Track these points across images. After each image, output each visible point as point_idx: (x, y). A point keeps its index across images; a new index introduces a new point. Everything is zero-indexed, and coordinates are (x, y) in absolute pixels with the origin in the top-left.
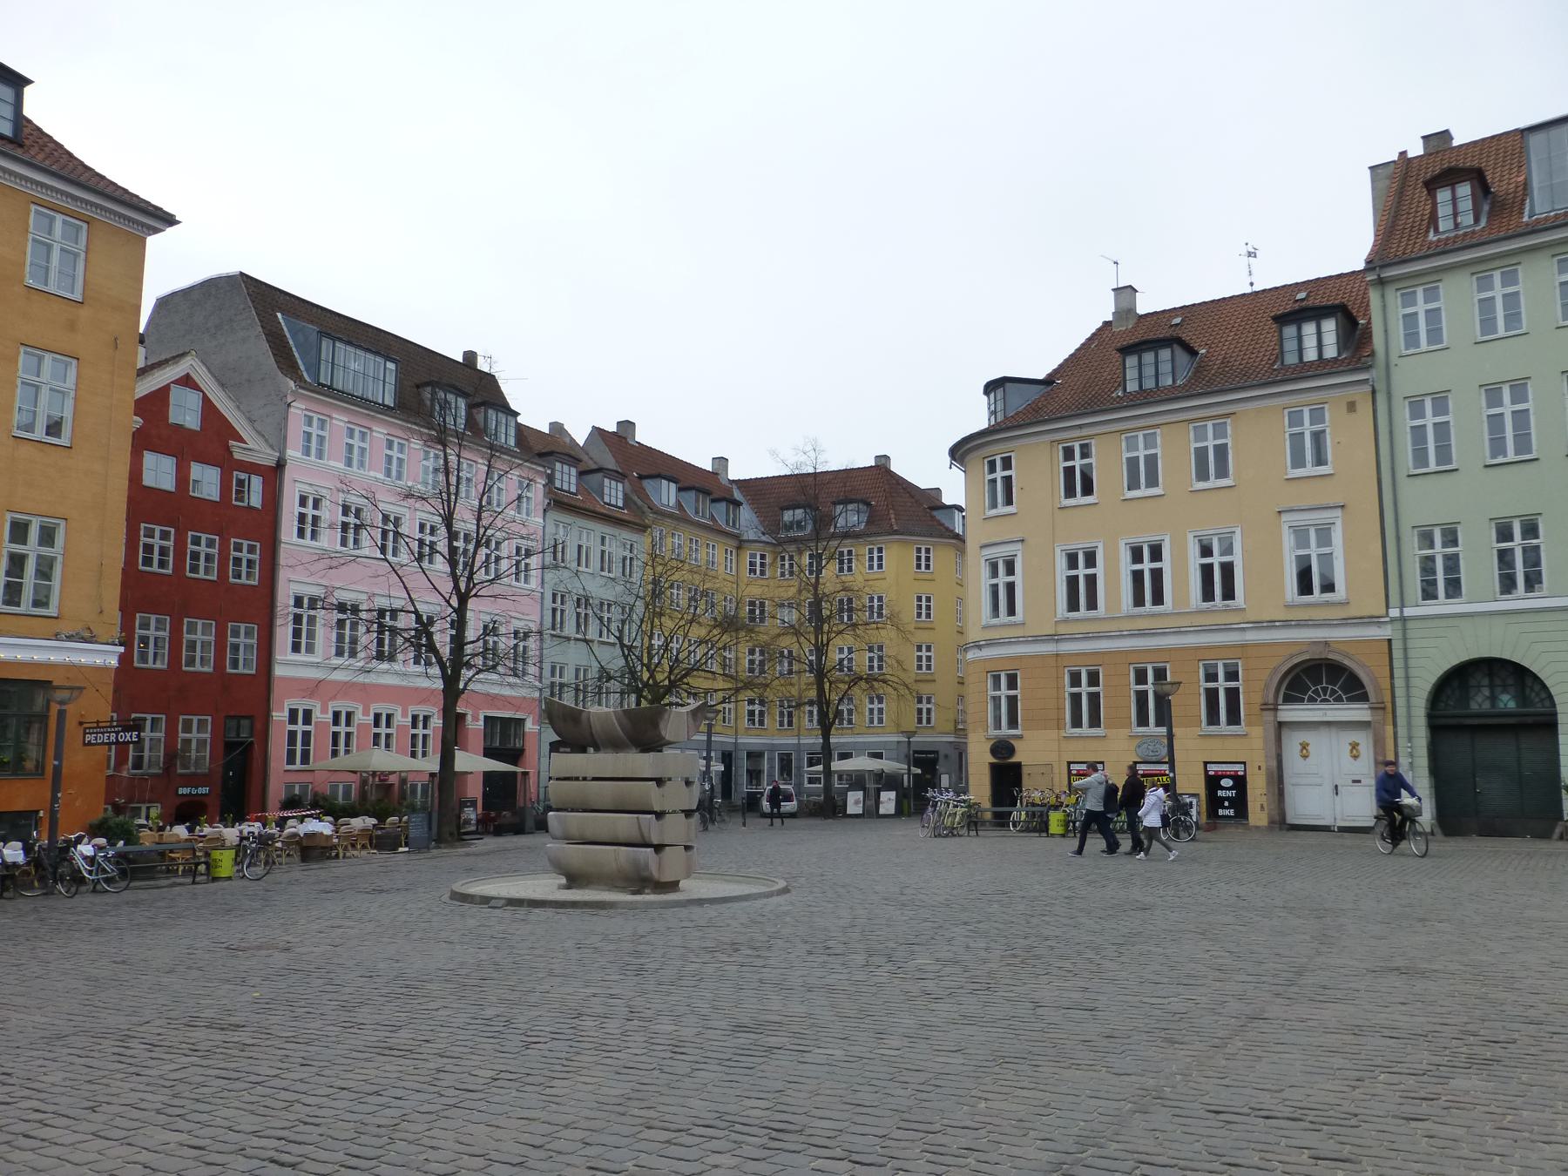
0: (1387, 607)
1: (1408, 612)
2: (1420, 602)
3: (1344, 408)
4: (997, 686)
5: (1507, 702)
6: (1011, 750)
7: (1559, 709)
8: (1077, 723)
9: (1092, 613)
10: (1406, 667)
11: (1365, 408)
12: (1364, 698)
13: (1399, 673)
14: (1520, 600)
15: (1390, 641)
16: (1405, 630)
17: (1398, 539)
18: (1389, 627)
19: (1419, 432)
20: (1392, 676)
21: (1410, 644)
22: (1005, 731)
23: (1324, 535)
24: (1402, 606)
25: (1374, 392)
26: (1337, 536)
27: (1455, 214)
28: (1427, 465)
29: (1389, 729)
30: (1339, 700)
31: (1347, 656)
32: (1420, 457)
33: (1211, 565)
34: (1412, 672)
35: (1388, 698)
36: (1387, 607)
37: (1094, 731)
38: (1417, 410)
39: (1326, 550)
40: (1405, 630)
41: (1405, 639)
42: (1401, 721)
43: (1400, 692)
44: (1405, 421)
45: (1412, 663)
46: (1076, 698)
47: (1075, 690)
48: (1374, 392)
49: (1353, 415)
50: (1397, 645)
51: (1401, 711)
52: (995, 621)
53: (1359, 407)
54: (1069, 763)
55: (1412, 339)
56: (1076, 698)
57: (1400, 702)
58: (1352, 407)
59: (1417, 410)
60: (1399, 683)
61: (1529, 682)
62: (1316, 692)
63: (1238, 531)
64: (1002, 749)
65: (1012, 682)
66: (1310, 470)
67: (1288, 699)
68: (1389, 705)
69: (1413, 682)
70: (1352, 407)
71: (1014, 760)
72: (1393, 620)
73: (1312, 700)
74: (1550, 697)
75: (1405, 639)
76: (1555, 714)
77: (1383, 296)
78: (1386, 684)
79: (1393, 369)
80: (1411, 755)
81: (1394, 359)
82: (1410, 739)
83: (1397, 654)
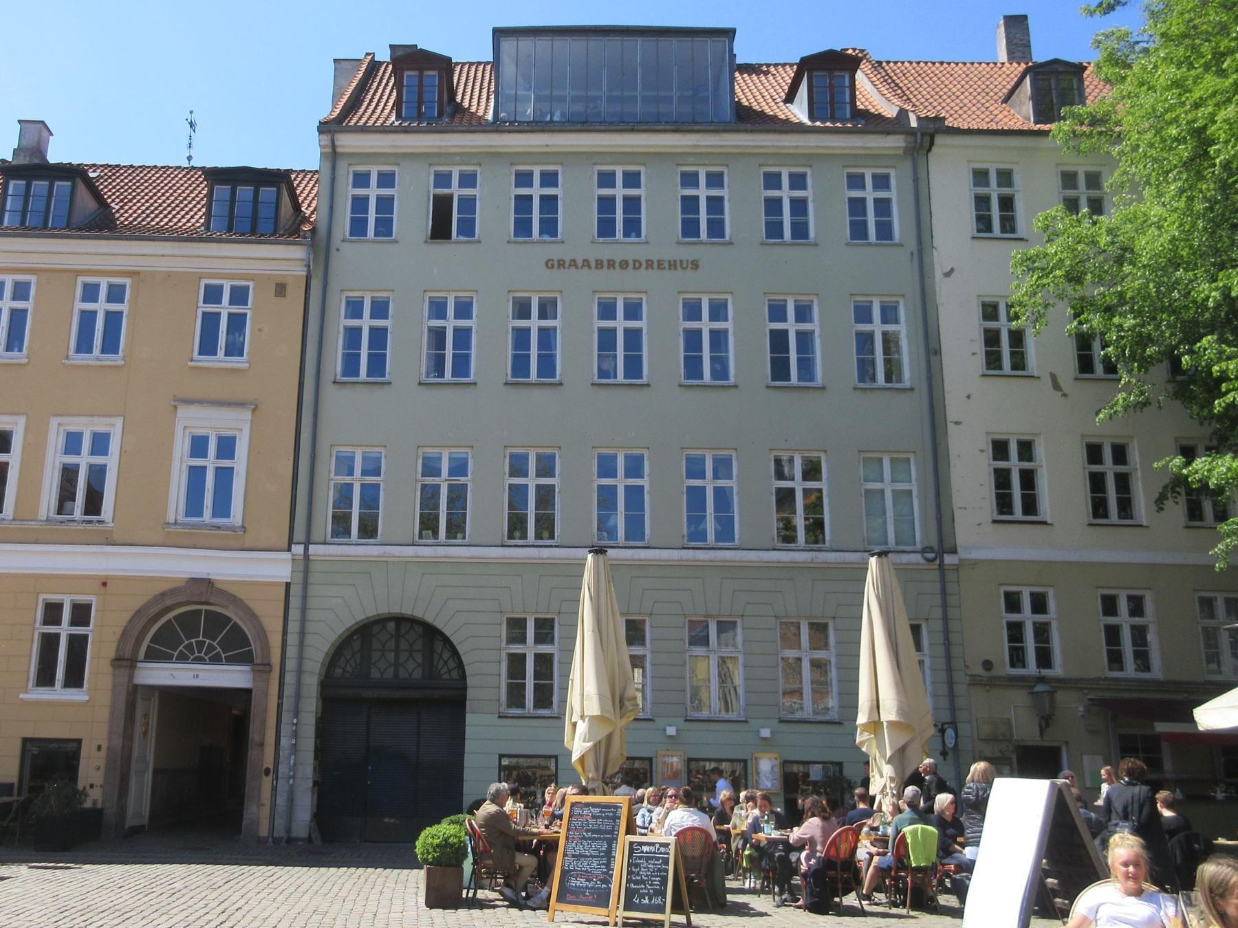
0: (291, 542)
3: (273, 288)
5: (413, 669)
7: (470, 681)
12: (244, 658)
13: (294, 627)
14: (439, 551)
15: (288, 585)
16: (307, 572)
19: (353, 336)
21: (312, 590)
23: (227, 447)
24: (307, 543)
25: (308, 278)
27: (420, 103)
28: (358, 375)
30: (216, 660)
31: (234, 600)
32: (351, 364)
34: (310, 627)
35: (276, 659)
36: (291, 542)
38: (355, 309)
39: (225, 463)
40: (307, 572)
41: (305, 584)
45: (311, 615)
50: (296, 591)
53: (289, 291)
55: (358, 227)
59: (355, 309)
61: (439, 646)
69: (309, 639)
70: (281, 290)
73: (182, 658)
74: (461, 666)
75: (305, 584)
76: (465, 688)
78: (275, 641)
79: (333, 250)
80: (295, 734)
82: (296, 713)
83: (295, 602)
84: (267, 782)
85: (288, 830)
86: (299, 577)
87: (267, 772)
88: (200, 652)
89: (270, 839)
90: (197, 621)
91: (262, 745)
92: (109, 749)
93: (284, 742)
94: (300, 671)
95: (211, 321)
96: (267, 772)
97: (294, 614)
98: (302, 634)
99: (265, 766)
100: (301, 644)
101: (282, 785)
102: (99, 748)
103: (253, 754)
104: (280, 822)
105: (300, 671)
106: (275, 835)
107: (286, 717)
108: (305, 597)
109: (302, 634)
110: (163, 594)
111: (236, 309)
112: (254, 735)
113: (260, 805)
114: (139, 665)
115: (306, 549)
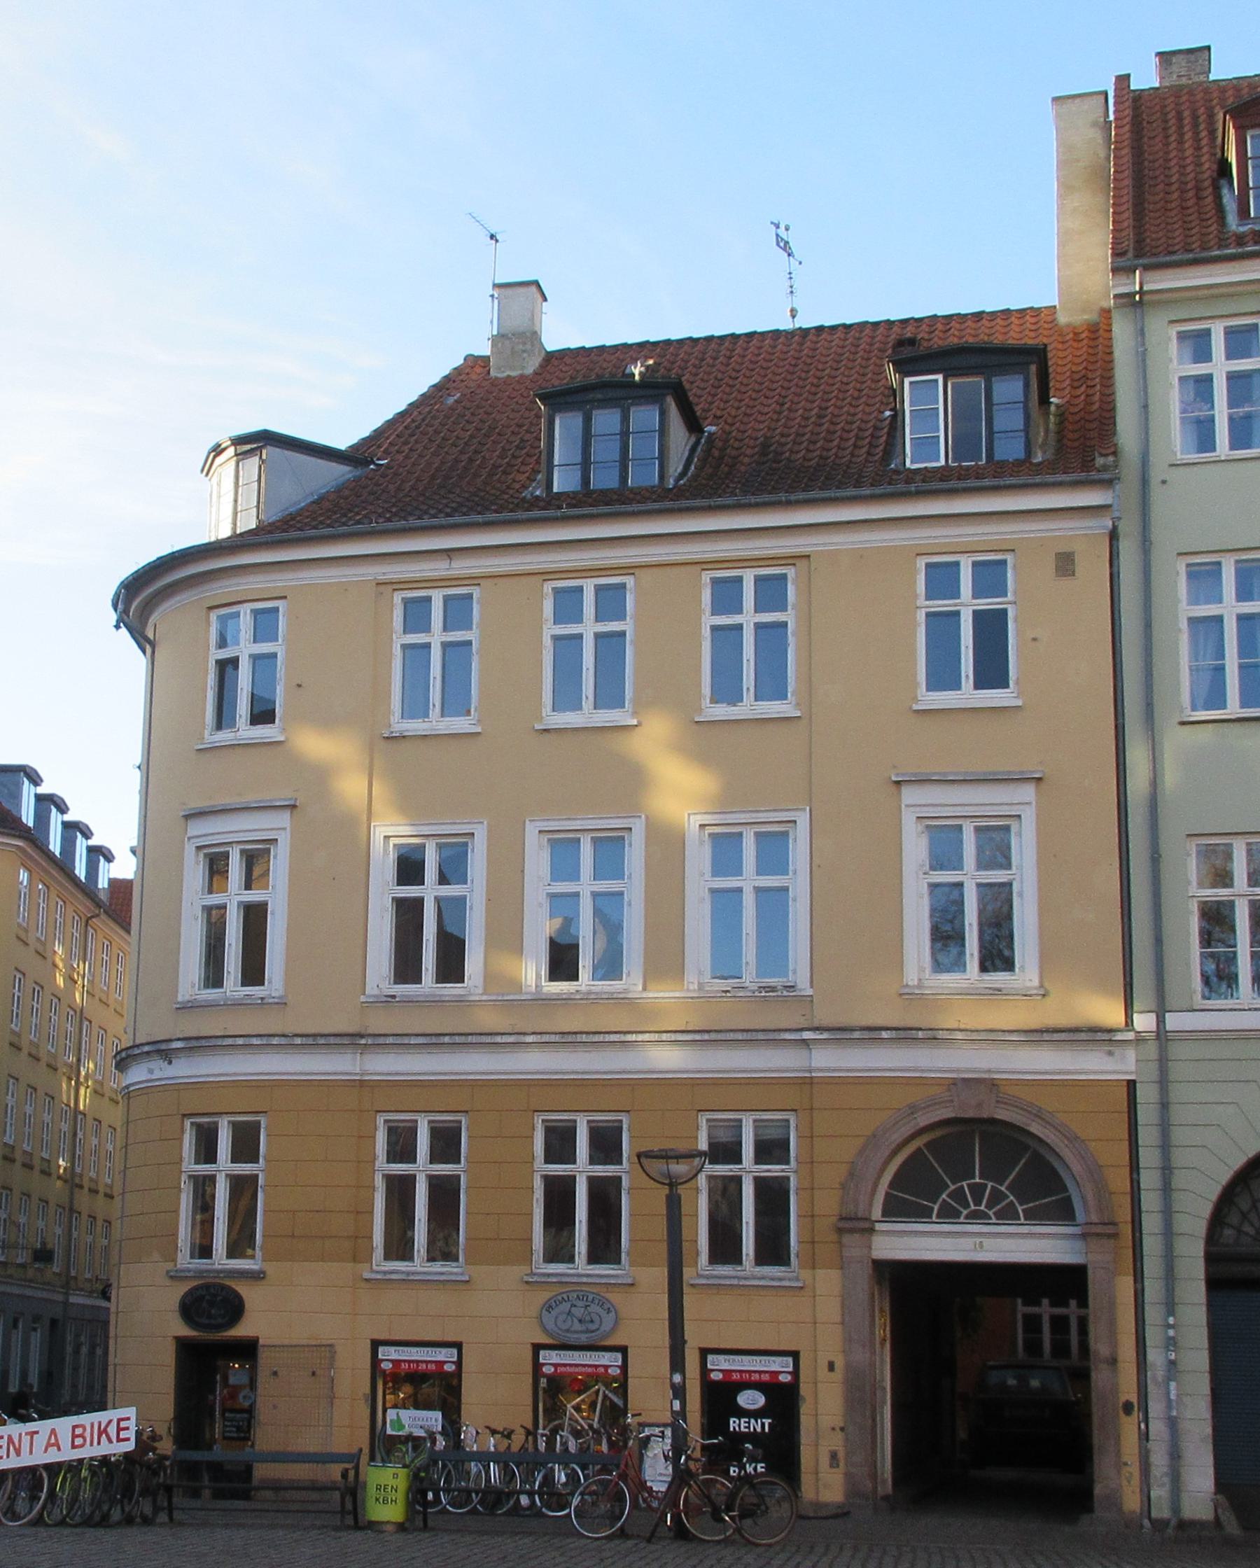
1: (1172, 1021)
2: (1198, 1001)
4: (207, 1151)
6: (234, 1309)
8: (399, 1247)
9: (451, 989)
10: (1165, 1146)
11: (1093, 568)
12: (1064, 1212)
13: (1149, 1157)
15: (1131, 1085)
16: (1163, 1061)
17: (1155, 859)
18: (1131, 1054)
20: (1134, 1166)
21: (1177, 1093)
22: (220, 1258)
23: (996, 848)
26: (1025, 847)
29: (1125, 1285)
31: (1039, 1115)
33: (418, 903)
34: (1180, 1157)
35: (1124, 1214)
37: (438, 1268)
39: (998, 876)
41: (1163, 1082)
42: (1153, 1266)
43: (1150, 1201)
44: (1180, 604)
45: (1179, 1136)
46: (400, 1189)
47: (400, 1168)
48: (1113, 536)
49: (1065, 583)
50: (1147, 1095)
51: (1152, 1245)
52: (212, 994)
54: (376, 1344)
56: (400, 1189)
57: (1151, 1223)
58: (1065, 564)
60: (1149, 1179)
62: (958, 1195)
63: (803, 820)
64: (212, 1304)
65: (246, 1147)
66: (968, 695)
67: (895, 1209)
68: (1127, 1230)
69: (1179, 1180)
70: (1065, 564)
71: (242, 1330)
72: (1140, 1040)
73: (948, 1213)
75: (1163, 1082)
77: (1141, 333)
78: (1119, 1181)
81: (1156, 475)
82: (1170, 1306)
83: (1147, 1114)
84: (1129, 1427)
85: (1176, 1507)
86: (1152, 1071)
87: (1128, 1408)
88: (989, 1206)
89: (1146, 1522)
90: (981, 1146)
91: (1113, 1361)
92: (848, 1367)
93: (1155, 1356)
94: (1168, 1233)
95: (942, 627)
96: (1128, 1408)
97: (1148, 1136)
98: (1167, 1170)
99: (1123, 1398)
100: (1167, 1189)
101: (1157, 1428)
102: (831, 1366)
103: (1099, 1377)
104: (1160, 1493)
105: (1168, 1233)
106: (1154, 1515)
107: (1153, 1314)
108: (1164, 1105)
109: (1167, 1170)
110: (913, 1109)
111: (985, 604)
112: (1099, 1347)
113: (1120, 1465)
114: (878, 1226)
115: (1161, 1021)
